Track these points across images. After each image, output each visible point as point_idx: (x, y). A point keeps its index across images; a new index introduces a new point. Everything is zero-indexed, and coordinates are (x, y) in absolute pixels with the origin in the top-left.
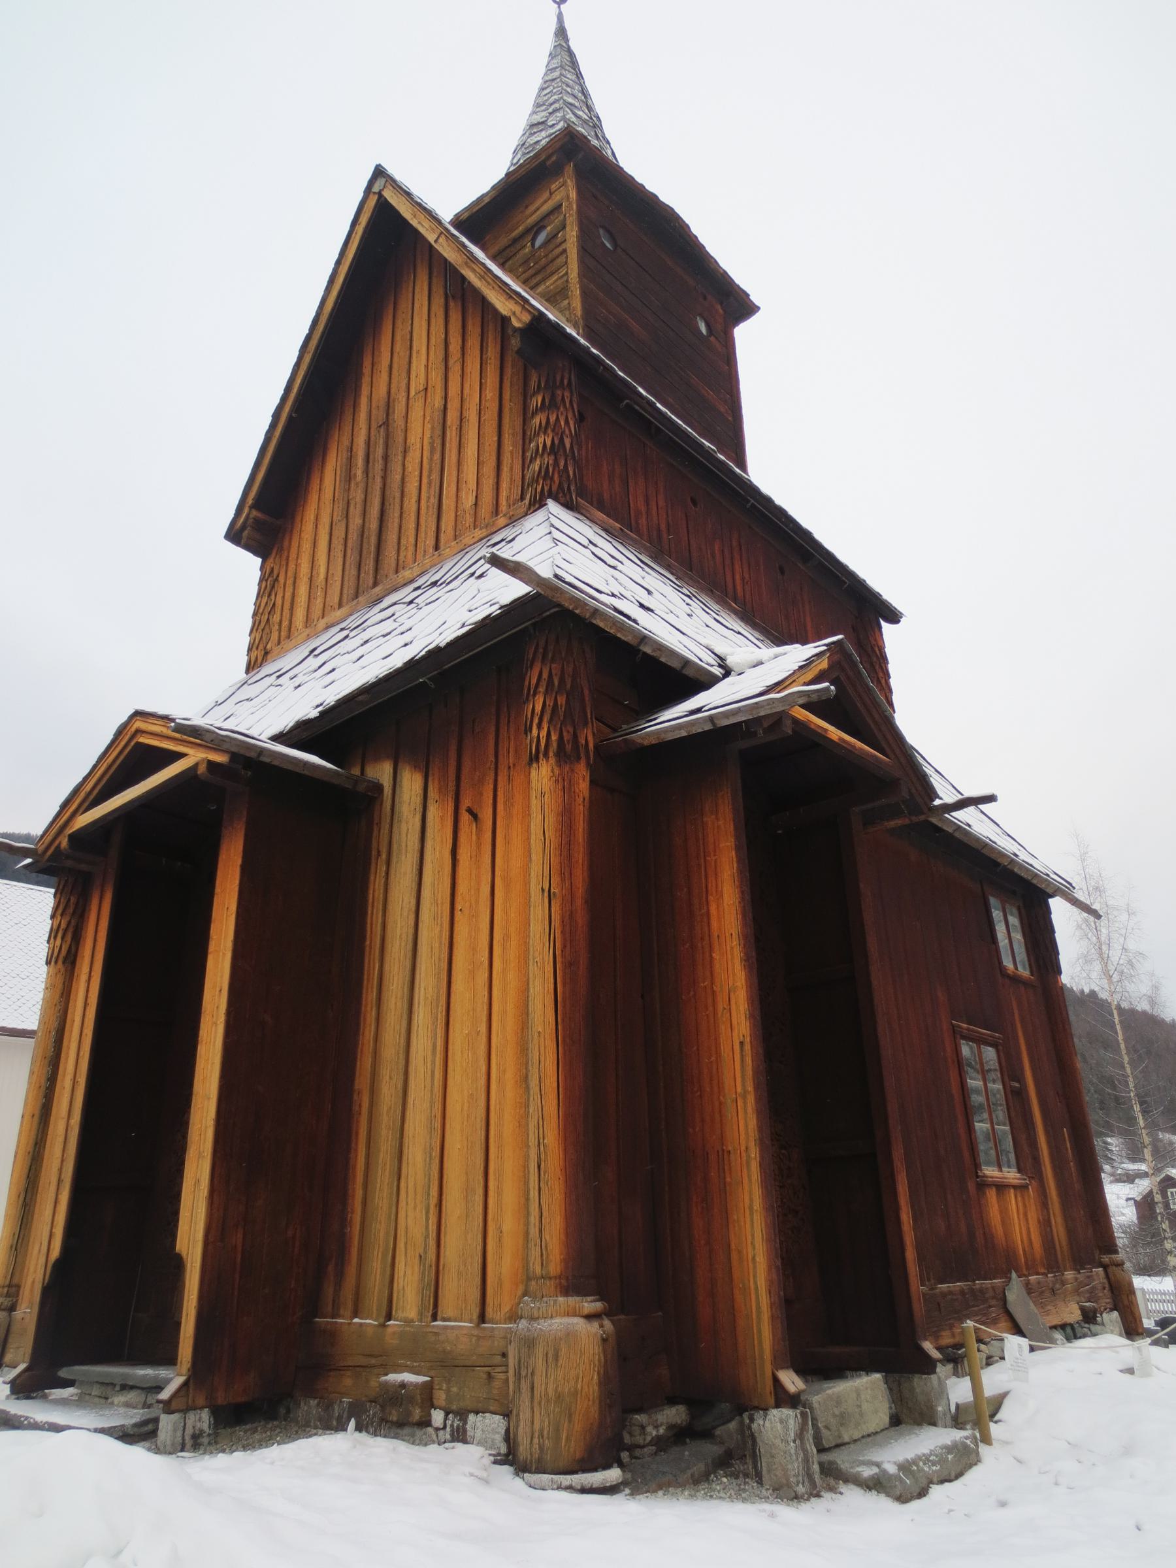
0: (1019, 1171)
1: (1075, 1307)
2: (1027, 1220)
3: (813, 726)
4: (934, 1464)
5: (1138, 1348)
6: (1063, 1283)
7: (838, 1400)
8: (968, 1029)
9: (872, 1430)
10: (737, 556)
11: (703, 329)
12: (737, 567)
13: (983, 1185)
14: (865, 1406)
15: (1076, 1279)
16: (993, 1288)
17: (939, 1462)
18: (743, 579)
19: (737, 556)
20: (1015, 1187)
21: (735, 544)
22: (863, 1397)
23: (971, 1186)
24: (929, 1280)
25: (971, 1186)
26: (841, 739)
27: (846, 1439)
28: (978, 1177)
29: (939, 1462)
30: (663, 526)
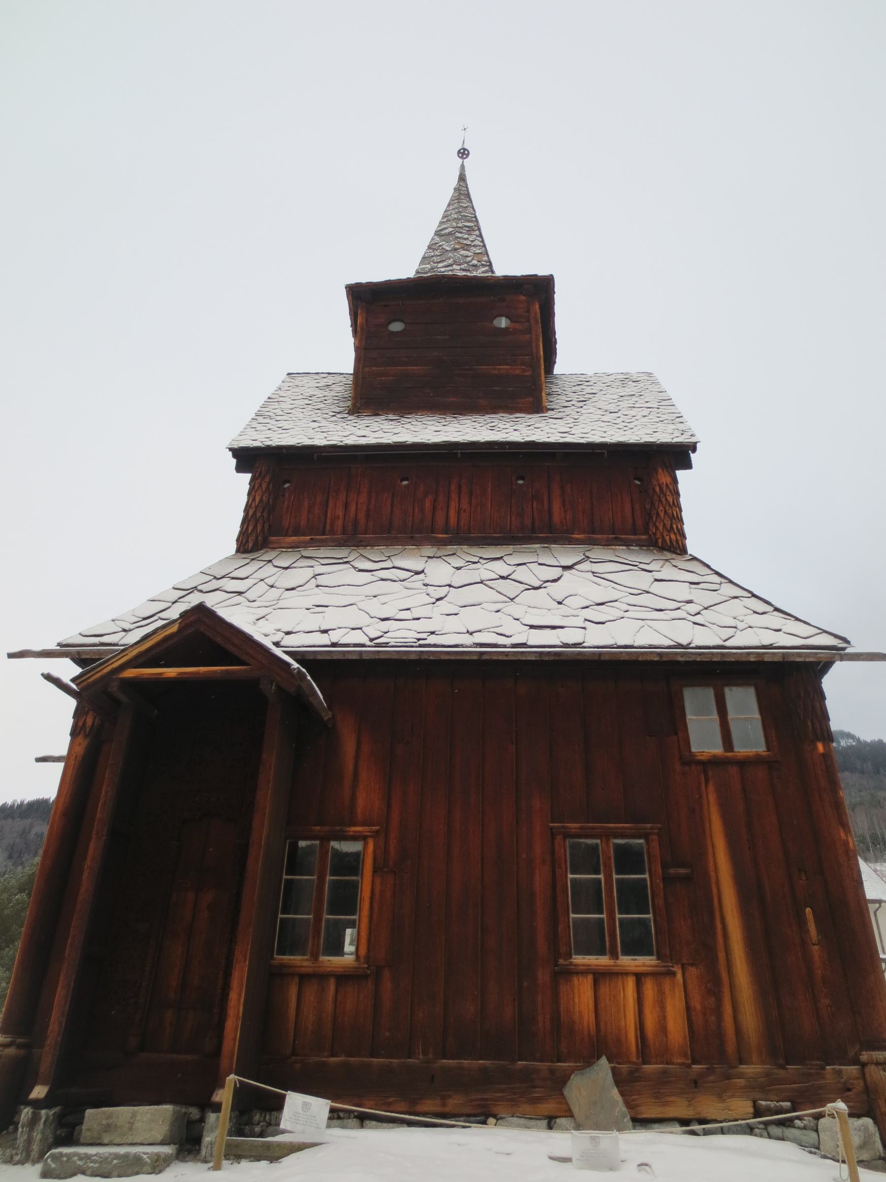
0: (658, 959)
1: (749, 1104)
2: (663, 1008)
3: (145, 676)
4: (93, 1161)
5: (593, 1139)
6: (728, 1077)
7: (109, 1117)
8: (581, 828)
9: (139, 1141)
10: (454, 496)
11: (503, 323)
12: (453, 505)
13: (570, 972)
14: (138, 1125)
15: (768, 1075)
16: (552, 1071)
17: (100, 1163)
18: (459, 512)
19: (454, 496)
20: (654, 975)
21: (453, 487)
22: (138, 1118)
23: (543, 976)
24: (425, 1053)
25: (543, 976)
26: (179, 674)
27: (106, 1141)
28: (556, 965)
29: (100, 1163)
30: (362, 516)
